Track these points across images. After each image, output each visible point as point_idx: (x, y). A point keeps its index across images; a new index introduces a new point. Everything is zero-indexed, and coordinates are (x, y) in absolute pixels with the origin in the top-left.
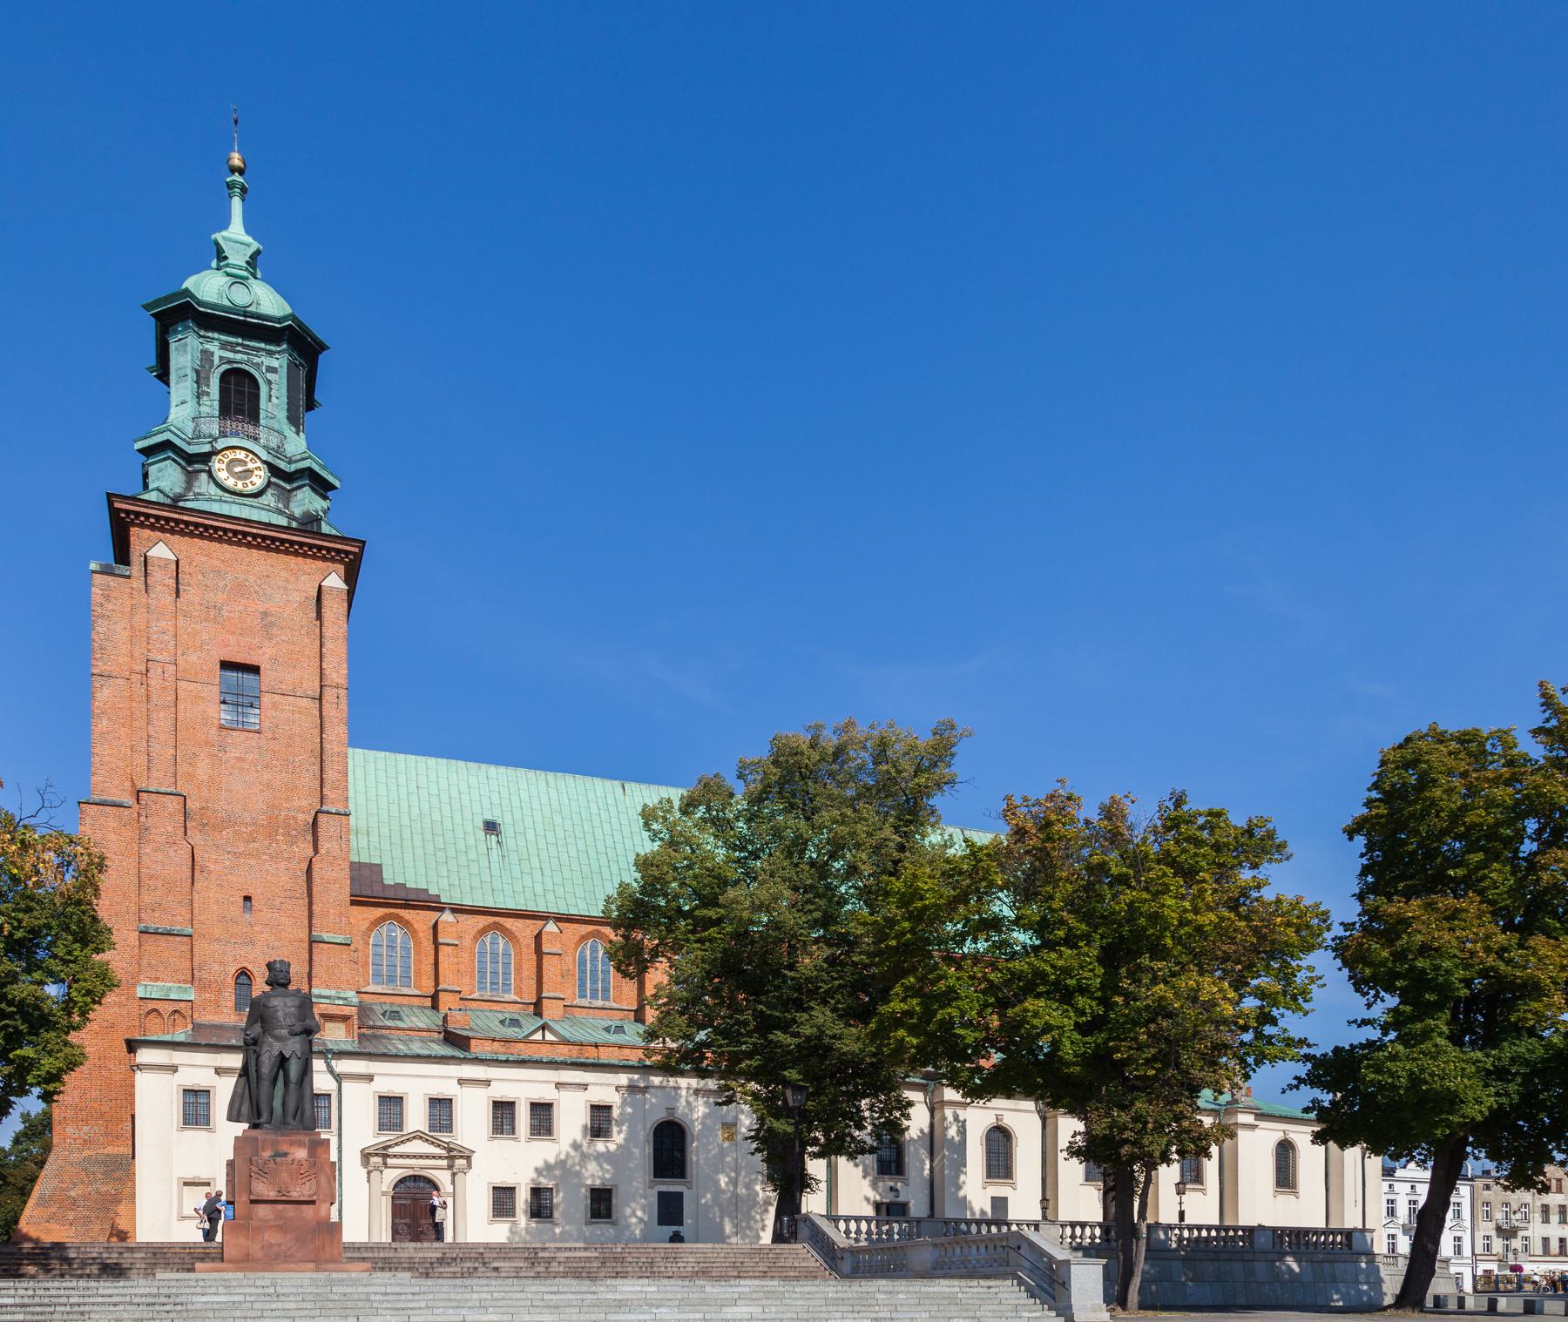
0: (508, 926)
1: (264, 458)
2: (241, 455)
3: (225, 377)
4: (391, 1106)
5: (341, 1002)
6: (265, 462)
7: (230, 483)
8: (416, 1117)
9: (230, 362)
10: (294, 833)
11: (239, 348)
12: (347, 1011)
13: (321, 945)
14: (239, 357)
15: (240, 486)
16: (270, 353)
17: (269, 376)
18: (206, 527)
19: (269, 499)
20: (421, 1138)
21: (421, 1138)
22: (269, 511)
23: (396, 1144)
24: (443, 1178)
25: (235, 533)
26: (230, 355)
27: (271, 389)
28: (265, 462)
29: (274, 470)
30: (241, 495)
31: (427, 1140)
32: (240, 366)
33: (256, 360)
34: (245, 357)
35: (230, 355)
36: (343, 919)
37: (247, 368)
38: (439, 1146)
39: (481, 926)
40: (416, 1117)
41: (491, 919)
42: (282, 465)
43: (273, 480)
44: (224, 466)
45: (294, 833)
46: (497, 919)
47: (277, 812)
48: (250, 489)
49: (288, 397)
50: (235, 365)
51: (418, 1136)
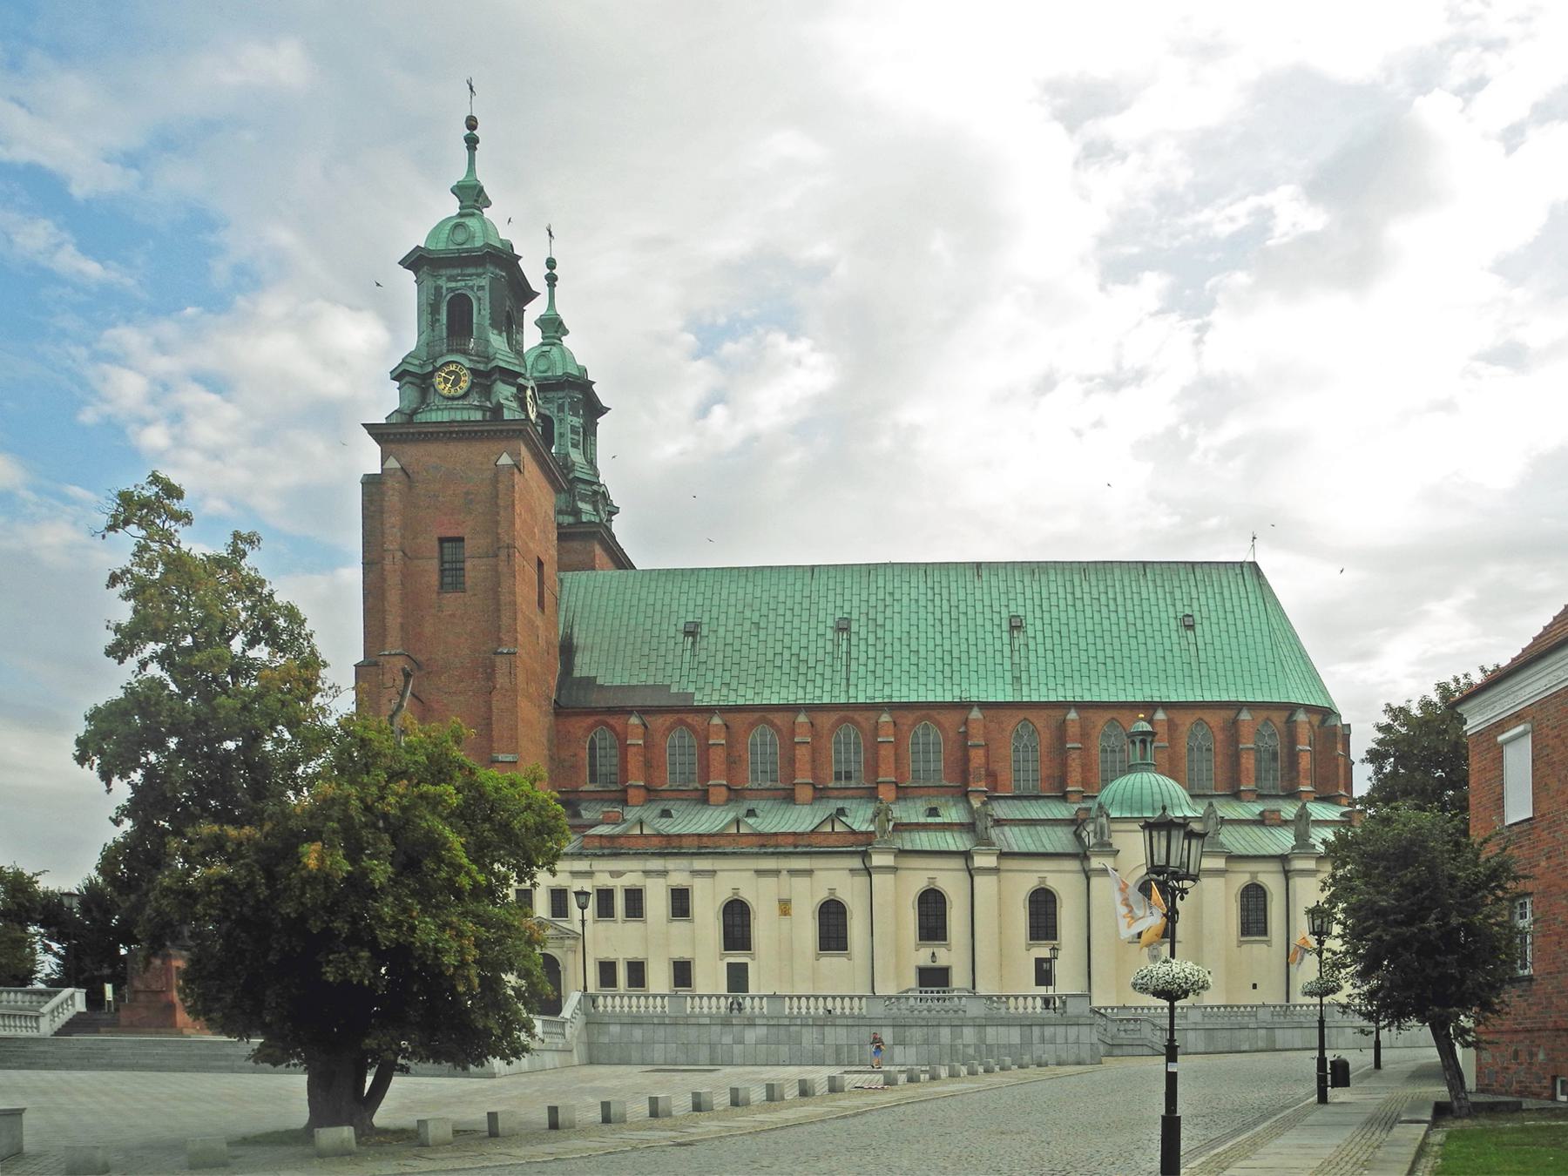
0: (689, 720)
1: (467, 366)
2: (452, 368)
3: (449, 303)
14: (460, 284)
17: (480, 294)
22: (468, 409)
25: (445, 433)
26: (453, 285)
29: (473, 371)
30: (453, 398)
33: (471, 283)
34: (463, 283)
35: (453, 285)
39: (668, 723)
41: (676, 717)
42: (481, 367)
46: (679, 715)
48: (460, 392)
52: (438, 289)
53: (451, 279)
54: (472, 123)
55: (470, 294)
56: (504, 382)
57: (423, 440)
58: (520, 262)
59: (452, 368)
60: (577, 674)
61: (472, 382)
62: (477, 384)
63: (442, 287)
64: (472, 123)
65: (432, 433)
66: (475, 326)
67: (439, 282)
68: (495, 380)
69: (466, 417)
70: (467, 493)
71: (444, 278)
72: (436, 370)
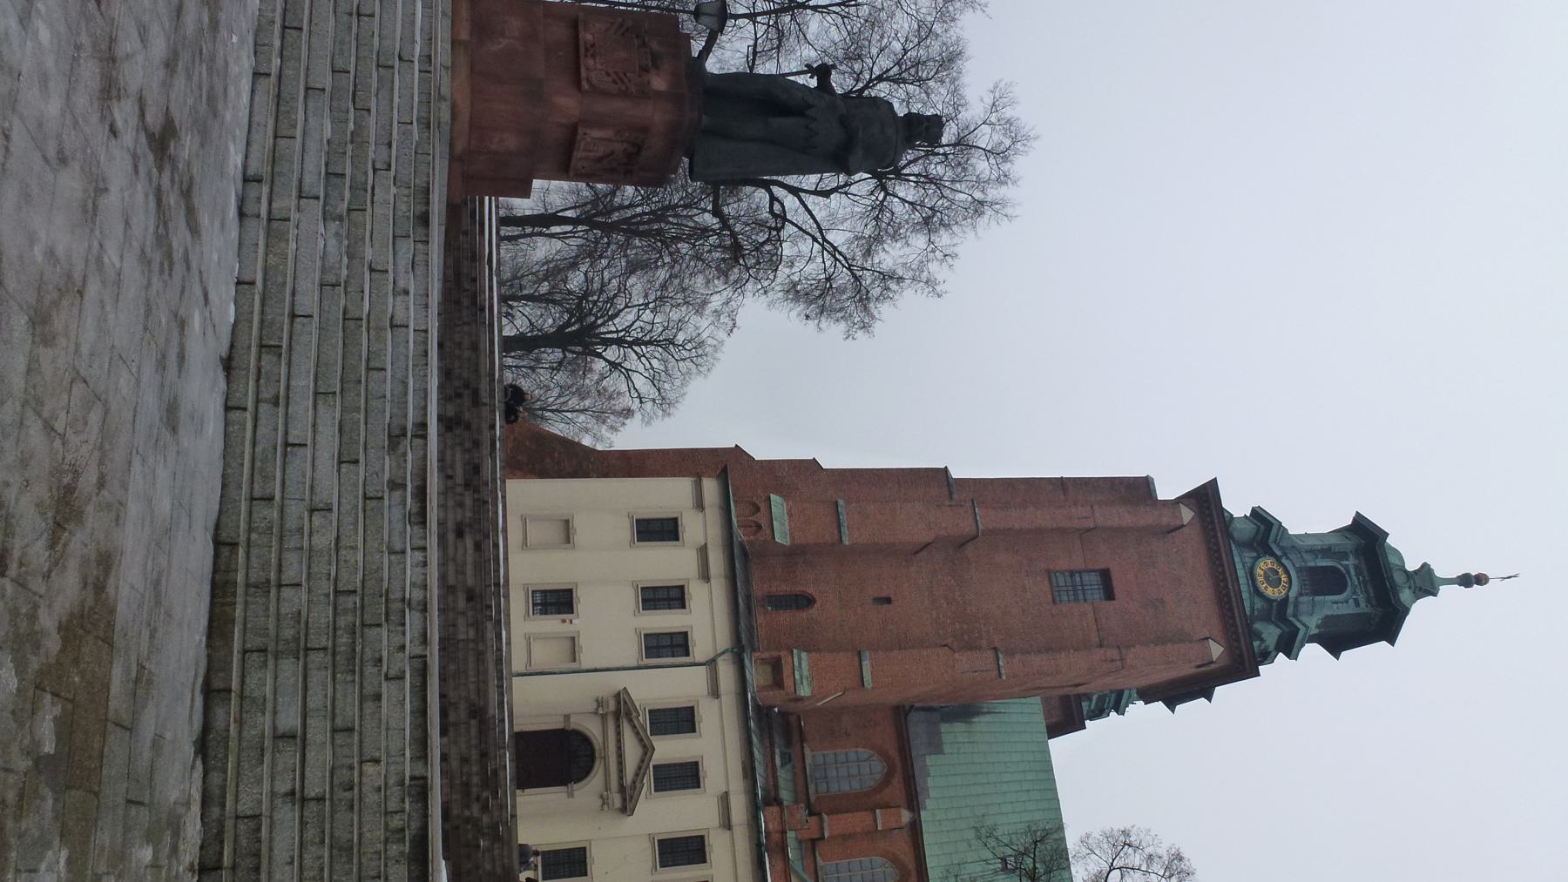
1: (1290, 594)
2: (1284, 578)
4: (680, 720)
5: (797, 677)
6: (1287, 596)
7: (1259, 572)
8: (669, 749)
9: (1349, 573)
10: (966, 638)
11: (1361, 578)
12: (788, 682)
13: (856, 659)
14: (1354, 578)
15: (1260, 579)
16: (1368, 601)
18: (1218, 550)
19: (1259, 604)
20: (646, 754)
21: (645, 754)
23: (634, 727)
24: (595, 782)
25: (1223, 573)
26: (1353, 572)
27: (1342, 603)
28: (1287, 596)
31: (642, 761)
32: (1348, 579)
33: (1358, 591)
34: (1356, 583)
35: (1353, 572)
36: (890, 679)
37: (1349, 584)
38: (637, 775)
40: (669, 749)
42: (1290, 610)
43: (1275, 604)
44: (1270, 566)
45: (966, 638)
47: (982, 621)
48: (1262, 587)
49: (1338, 615)
50: (1347, 576)
51: (647, 750)
52: (1343, 555)
53: (1357, 568)
54: (1481, 580)
55: (1349, 591)
56: (1280, 637)
57: (1209, 549)
58: (1384, 643)
59: (1284, 578)
60: (944, 727)
61: (1274, 601)
62: (1272, 606)
63: (1347, 560)
64: (1481, 580)
65: (1220, 558)
66: (1322, 597)
67: (1351, 558)
68: (1278, 626)
69: (1244, 596)
70: (1162, 602)
71: (1357, 562)
72: (1278, 559)
